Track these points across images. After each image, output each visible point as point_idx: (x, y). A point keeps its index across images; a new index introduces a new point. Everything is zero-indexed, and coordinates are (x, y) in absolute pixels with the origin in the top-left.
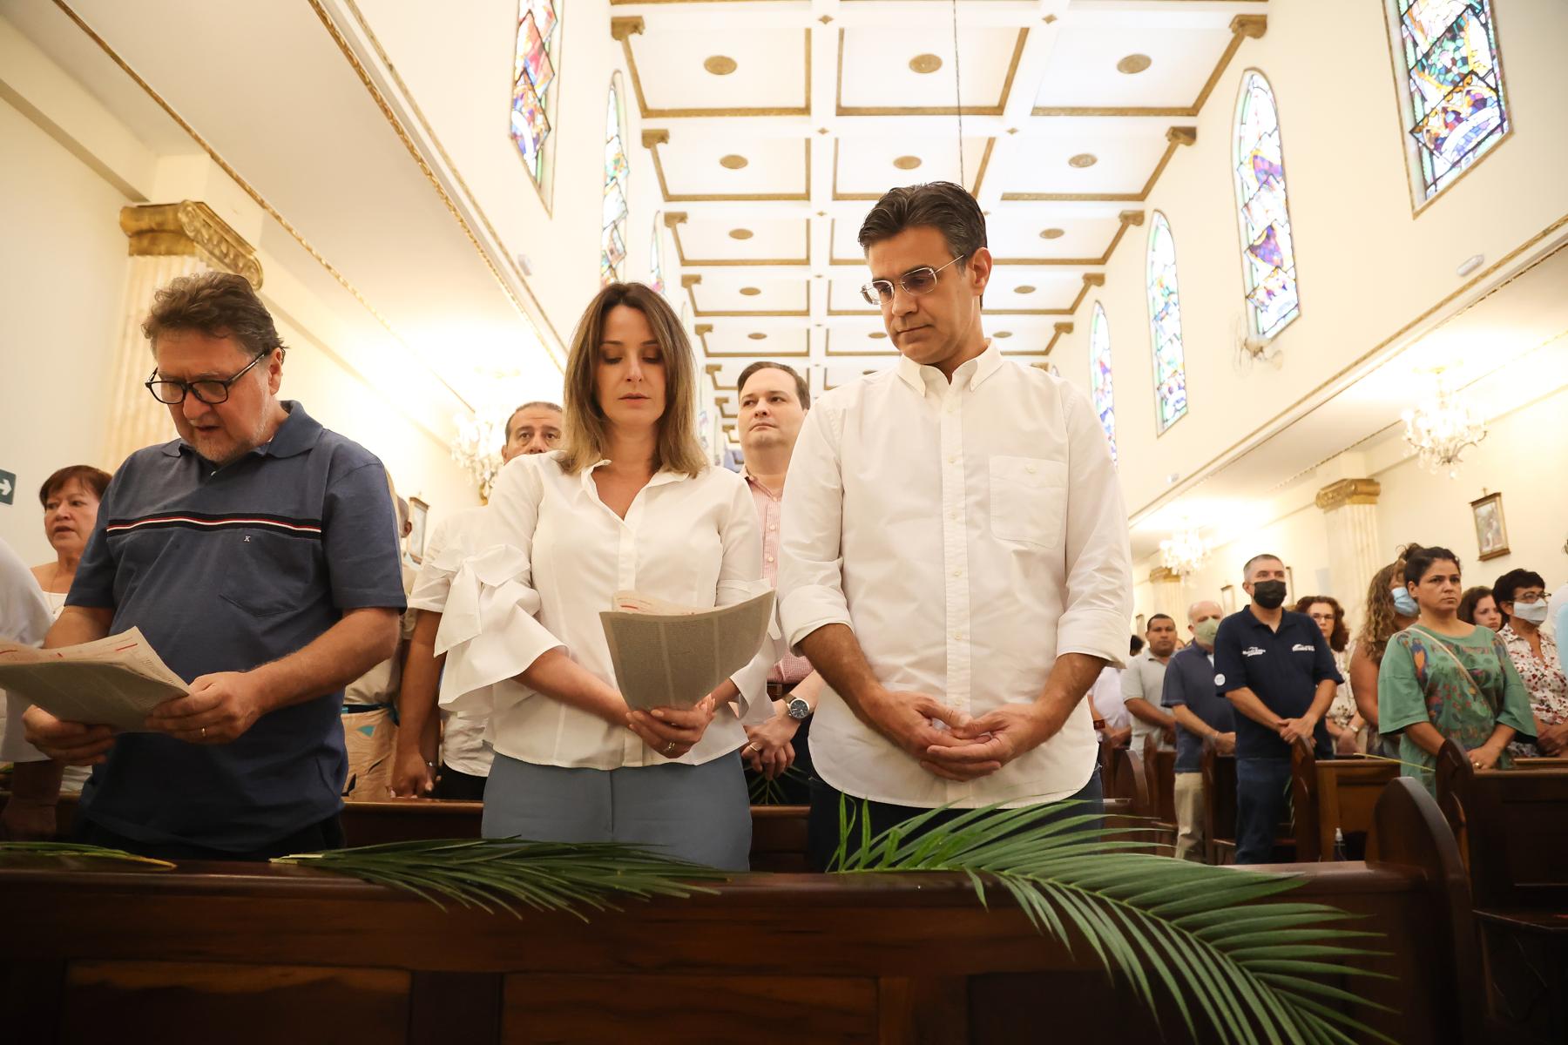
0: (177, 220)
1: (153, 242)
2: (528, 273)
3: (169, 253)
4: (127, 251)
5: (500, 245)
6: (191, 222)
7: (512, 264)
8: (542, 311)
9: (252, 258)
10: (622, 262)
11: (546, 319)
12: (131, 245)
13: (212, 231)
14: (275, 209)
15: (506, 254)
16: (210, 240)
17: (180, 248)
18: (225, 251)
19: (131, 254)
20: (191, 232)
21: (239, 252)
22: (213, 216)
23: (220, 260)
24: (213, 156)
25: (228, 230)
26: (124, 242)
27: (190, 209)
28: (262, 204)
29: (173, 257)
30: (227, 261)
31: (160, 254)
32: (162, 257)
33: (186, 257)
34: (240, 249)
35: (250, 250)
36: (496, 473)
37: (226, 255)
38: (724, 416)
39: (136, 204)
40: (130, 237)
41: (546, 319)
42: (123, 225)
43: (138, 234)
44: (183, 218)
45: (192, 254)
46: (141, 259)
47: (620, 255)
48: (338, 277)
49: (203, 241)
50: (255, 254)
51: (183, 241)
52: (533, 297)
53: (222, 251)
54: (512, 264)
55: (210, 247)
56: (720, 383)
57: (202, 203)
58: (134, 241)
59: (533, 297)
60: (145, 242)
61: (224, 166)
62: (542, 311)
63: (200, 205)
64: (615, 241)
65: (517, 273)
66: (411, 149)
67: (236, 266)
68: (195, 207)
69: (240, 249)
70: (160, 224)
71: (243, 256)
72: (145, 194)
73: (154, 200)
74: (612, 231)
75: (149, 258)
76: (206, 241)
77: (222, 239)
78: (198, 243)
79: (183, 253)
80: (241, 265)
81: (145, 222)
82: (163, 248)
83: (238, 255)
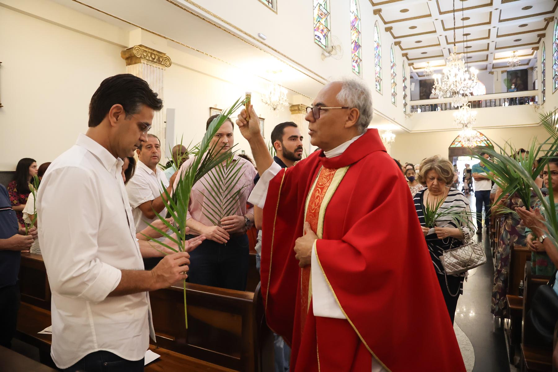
0: (133, 53)
1: (131, 59)
2: (264, 39)
3: (135, 63)
4: (126, 65)
5: (246, 34)
6: (138, 52)
7: (254, 38)
8: (276, 51)
9: (166, 56)
10: (329, 17)
11: (279, 53)
12: (126, 62)
13: (147, 52)
14: (170, 38)
15: (250, 36)
16: (147, 55)
17: (137, 61)
18: (154, 57)
19: (127, 66)
20: (139, 56)
21: (159, 56)
22: (147, 48)
23: (152, 61)
24: (142, 28)
25: (154, 50)
26: (124, 62)
27: (136, 48)
28: (165, 37)
29: (136, 64)
30: (155, 60)
31: (133, 64)
32: (134, 65)
33: (139, 63)
34: (161, 55)
35: (165, 54)
36: (276, 108)
37: (154, 59)
38: (408, 59)
39: (126, 49)
40: (126, 60)
41: (279, 53)
42: (122, 57)
43: (127, 59)
44: (135, 52)
45: (140, 62)
46: (128, 66)
47: (326, 15)
48: (203, 53)
49: (144, 57)
50: (166, 55)
51: (138, 59)
52: (269, 47)
53: (152, 58)
54: (254, 38)
55: (147, 58)
56: (403, 48)
57: (141, 45)
58: (127, 61)
59: (269, 47)
60: (129, 61)
61: (146, 30)
62: (276, 51)
63: (141, 46)
64: (322, 10)
65: (258, 40)
66: (192, 13)
67: (159, 61)
68: (139, 47)
69: (161, 55)
70: (130, 55)
71: (161, 57)
72: (128, 46)
73: (130, 47)
74: (319, 7)
75: (131, 65)
76: (145, 57)
77: (152, 54)
78: (142, 58)
79: (138, 63)
80: (161, 60)
81: (127, 56)
82: (134, 62)
83: (159, 58)
